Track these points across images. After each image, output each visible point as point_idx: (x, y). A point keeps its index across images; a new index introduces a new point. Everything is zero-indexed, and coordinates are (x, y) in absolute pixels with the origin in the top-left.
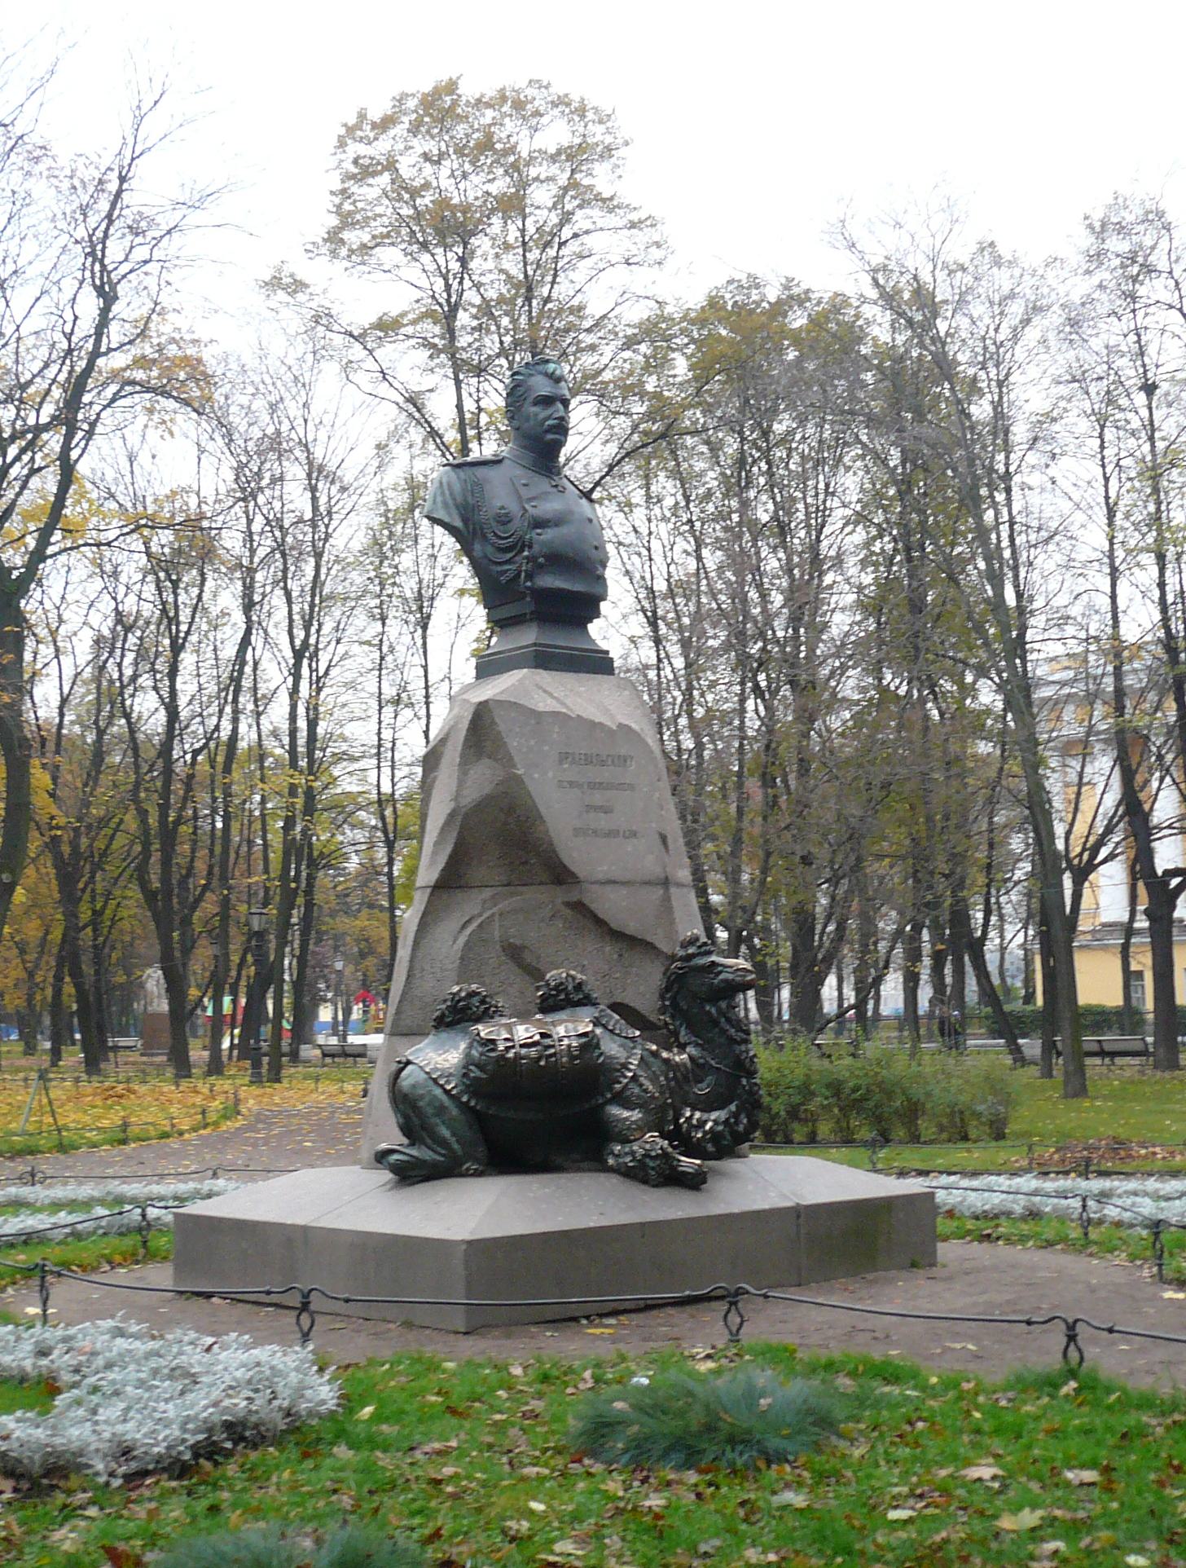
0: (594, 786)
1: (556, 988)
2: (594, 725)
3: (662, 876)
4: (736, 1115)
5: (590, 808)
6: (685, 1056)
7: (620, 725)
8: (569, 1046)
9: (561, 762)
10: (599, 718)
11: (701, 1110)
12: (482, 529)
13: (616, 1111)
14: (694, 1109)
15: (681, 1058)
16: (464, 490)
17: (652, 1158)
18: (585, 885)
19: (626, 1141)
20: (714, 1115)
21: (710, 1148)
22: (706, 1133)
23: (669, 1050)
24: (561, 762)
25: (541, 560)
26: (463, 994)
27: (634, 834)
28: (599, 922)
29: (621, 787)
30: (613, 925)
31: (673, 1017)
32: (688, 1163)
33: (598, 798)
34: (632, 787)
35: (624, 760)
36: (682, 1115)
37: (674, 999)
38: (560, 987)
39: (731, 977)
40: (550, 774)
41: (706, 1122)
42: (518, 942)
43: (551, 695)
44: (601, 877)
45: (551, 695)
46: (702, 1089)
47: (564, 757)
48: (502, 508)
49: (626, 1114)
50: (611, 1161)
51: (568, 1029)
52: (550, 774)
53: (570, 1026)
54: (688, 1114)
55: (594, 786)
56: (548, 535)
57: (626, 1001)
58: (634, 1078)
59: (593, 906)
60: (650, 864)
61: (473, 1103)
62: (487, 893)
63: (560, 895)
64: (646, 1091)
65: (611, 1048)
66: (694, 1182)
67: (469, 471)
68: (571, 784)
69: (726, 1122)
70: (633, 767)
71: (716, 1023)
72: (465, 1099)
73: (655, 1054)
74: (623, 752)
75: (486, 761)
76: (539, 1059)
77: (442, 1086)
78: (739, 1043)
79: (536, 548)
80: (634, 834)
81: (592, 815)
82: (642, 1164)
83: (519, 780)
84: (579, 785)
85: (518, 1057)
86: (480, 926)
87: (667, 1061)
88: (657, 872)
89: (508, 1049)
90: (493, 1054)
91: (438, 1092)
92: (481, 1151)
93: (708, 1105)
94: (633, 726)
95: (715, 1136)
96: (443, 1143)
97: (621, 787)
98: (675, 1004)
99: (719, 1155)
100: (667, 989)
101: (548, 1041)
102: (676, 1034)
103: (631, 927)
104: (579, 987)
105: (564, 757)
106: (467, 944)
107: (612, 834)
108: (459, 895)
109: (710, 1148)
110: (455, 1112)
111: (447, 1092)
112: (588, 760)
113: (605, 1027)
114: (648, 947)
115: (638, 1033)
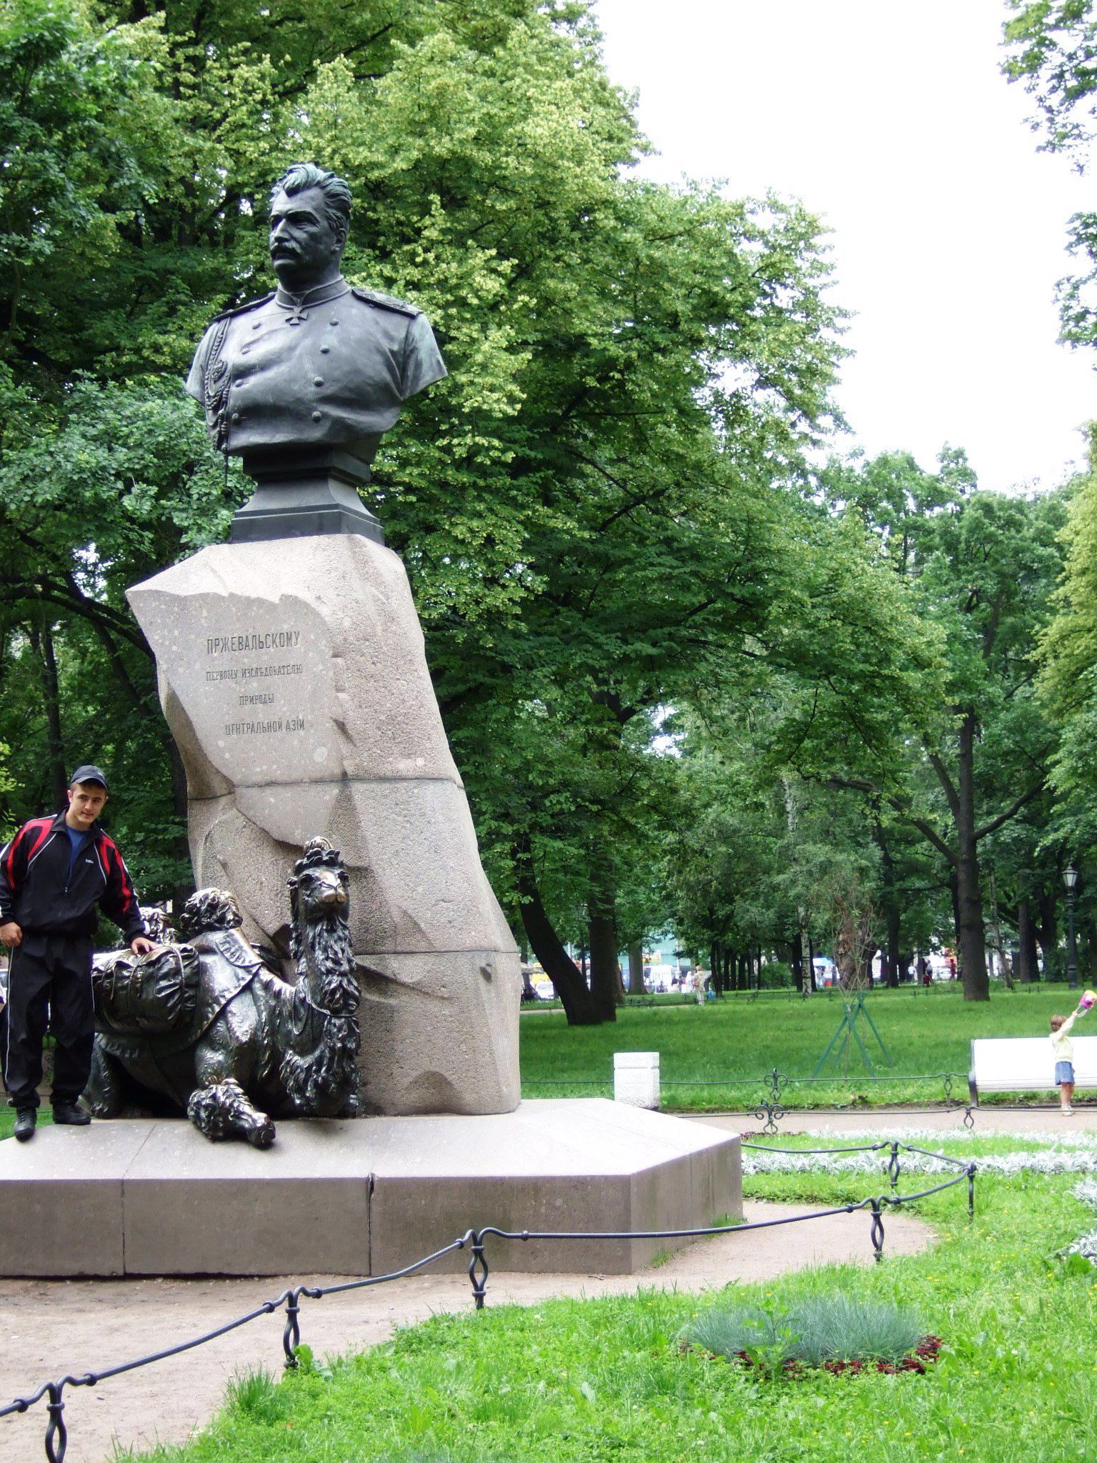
0: (248, 672)
2: (249, 602)
3: (337, 771)
4: (319, 1062)
7: (285, 598)
9: (210, 651)
14: (296, 1053)
18: (238, 790)
24: (210, 651)
25: (235, 416)
33: (254, 686)
36: (284, 1057)
40: (197, 666)
47: (213, 644)
52: (197, 666)
55: (248, 672)
56: (252, 382)
62: (223, 801)
65: (223, 978)
66: (263, 1141)
68: (223, 675)
70: (299, 646)
73: (267, 986)
74: (286, 628)
79: (231, 402)
81: (248, 707)
104: (213, 906)
105: (213, 644)
107: (270, 727)
112: (242, 644)
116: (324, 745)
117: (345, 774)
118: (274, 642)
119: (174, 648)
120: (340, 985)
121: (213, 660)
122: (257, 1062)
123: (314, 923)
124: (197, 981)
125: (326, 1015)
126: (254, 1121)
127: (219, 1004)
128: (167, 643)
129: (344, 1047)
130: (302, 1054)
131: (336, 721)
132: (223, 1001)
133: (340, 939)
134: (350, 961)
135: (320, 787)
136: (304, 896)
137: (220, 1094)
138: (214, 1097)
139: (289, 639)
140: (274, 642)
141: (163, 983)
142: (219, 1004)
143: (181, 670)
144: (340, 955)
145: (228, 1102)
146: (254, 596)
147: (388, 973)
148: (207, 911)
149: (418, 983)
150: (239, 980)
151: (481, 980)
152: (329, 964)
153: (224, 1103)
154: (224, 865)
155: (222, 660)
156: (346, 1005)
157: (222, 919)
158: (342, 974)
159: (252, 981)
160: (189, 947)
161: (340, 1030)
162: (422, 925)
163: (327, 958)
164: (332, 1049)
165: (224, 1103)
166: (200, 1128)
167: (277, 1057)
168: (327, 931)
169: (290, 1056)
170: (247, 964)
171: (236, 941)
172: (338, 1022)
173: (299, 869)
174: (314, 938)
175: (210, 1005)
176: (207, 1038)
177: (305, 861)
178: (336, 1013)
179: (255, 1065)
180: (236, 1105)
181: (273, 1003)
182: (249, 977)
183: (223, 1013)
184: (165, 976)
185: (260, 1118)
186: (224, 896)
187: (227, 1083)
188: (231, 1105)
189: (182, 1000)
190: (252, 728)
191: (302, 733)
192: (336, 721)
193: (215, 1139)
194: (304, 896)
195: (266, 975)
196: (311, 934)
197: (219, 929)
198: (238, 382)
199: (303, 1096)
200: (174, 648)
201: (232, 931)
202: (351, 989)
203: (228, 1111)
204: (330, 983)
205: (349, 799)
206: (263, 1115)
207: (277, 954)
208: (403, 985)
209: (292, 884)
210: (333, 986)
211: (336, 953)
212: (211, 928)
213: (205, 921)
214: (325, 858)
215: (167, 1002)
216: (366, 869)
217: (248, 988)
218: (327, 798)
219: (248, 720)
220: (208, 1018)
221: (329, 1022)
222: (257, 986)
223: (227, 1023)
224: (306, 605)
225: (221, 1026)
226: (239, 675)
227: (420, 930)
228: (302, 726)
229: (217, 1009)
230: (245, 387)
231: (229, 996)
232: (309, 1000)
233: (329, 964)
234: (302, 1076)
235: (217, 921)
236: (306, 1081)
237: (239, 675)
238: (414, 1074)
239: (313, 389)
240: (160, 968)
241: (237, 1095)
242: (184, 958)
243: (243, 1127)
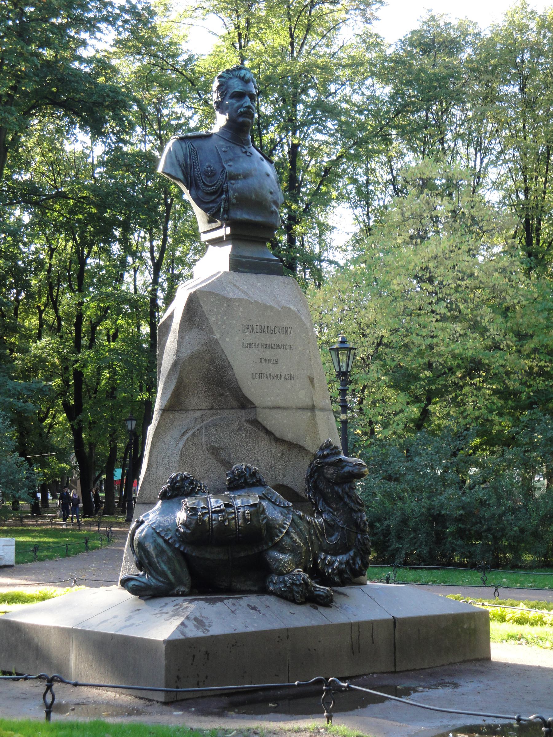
0: (265, 346)
1: (239, 475)
2: (266, 307)
4: (354, 558)
5: (262, 360)
6: (321, 520)
7: (283, 308)
8: (244, 513)
9: (244, 331)
10: (270, 303)
11: (331, 555)
12: (196, 181)
13: (276, 554)
14: (327, 553)
15: (319, 521)
16: (185, 156)
17: (296, 585)
18: (258, 410)
19: (281, 574)
20: (339, 558)
21: (337, 579)
22: (333, 570)
23: (312, 515)
24: (244, 331)
26: (178, 478)
27: (292, 377)
28: (268, 433)
29: (282, 347)
30: (278, 435)
31: (314, 495)
32: (322, 589)
33: (268, 354)
34: (291, 347)
35: (286, 330)
37: (315, 482)
38: (241, 474)
39: (351, 469)
40: (237, 338)
41: (334, 562)
42: (217, 445)
43: (238, 288)
44: (269, 404)
45: (238, 288)
47: (246, 327)
48: (209, 166)
49: (281, 556)
50: (271, 587)
51: (244, 501)
52: (237, 338)
53: (245, 499)
55: (265, 346)
57: (285, 483)
58: (288, 533)
59: (264, 423)
60: (302, 397)
61: (182, 549)
63: (243, 415)
64: (295, 542)
65: (274, 514)
67: (188, 142)
69: (347, 562)
71: (341, 499)
72: (177, 546)
74: (285, 324)
75: (196, 330)
76: (224, 521)
77: (163, 538)
78: (356, 512)
80: (292, 377)
81: (264, 364)
82: (291, 590)
83: (216, 342)
84: (256, 346)
85: (211, 520)
86: (193, 434)
87: (309, 523)
88: (307, 402)
89: (204, 514)
90: (195, 518)
91: (160, 541)
92: (187, 579)
93: (335, 551)
94: (293, 308)
95: (340, 572)
96: (163, 574)
97: (282, 347)
98: (316, 487)
99: (343, 583)
100: (311, 476)
101: (231, 510)
102: (316, 505)
103: (290, 436)
104: (254, 474)
105: (246, 327)
106: (184, 446)
107: (276, 377)
108: (180, 415)
109: (337, 579)
110: (170, 553)
111: (166, 541)
112: (262, 329)
113: (269, 500)
114: (300, 448)
115: (291, 504)
116: (304, 389)
117: (313, 405)
118: (279, 331)
119: (224, 327)
121: (246, 336)
126: (328, 591)
127: (284, 528)
128: (220, 323)
131: (309, 377)
135: (301, 412)
138: (303, 579)
139: (287, 330)
140: (279, 331)
142: (284, 528)
143: (227, 339)
146: (268, 304)
148: (250, 475)
155: (250, 338)
187: (299, 571)
190: (266, 376)
191: (293, 381)
192: (309, 377)
193: (301, 603)
197: (258, 486)
198: (233, 182)
200: (224, 327)
205: (315, 419)
209: (318, 463)
212: (253, 485)
217: (293, 520)
218: (305, 417)
219: (264, 372)
224: (296, 314)
226: (260, 346)
228: (293, 378)
229: (285, 531)
230: (234, 186)
237: (260, 346)
239: (270, 195)
243: (319, 596)
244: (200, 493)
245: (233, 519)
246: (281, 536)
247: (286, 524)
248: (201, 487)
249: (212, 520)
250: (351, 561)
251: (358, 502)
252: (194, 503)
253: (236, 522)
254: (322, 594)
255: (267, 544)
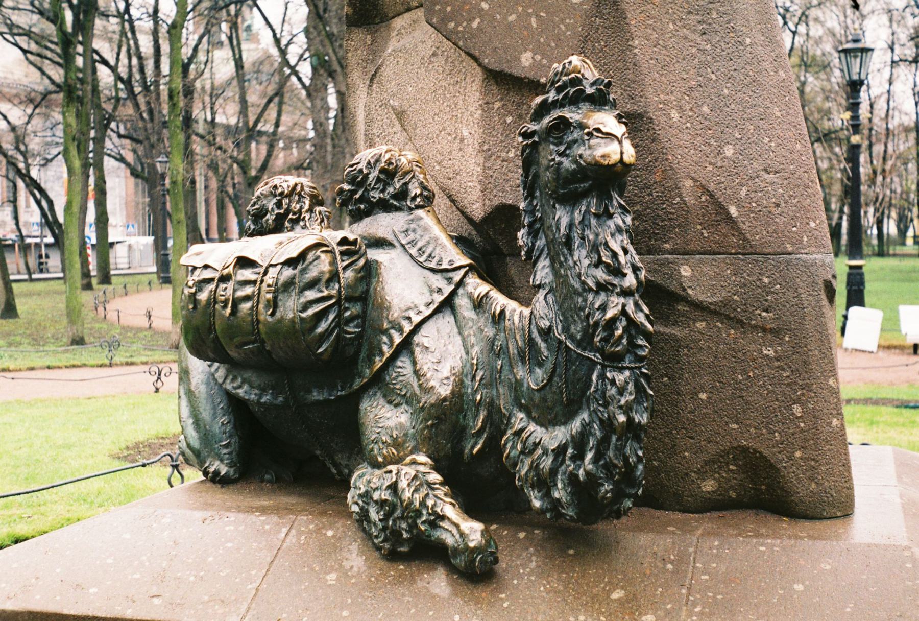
4: (579, 442)
19: (376, 465)
46: (533, 379)
54: (518, 427)
65: (404, 288)
69: (560, 451)
73: (479, 304)
85: (213, 300)
95: (544, 483)
101: (247, 274)
104: (389, 174)
120: (623, 312)
122: (464, 429)
123: (571, 200)
124: (363, 293)
125: (595, 363)
127: (400, 330)
129: (630, 420)
130: (547, 422)
132: (408, 328)
133: (619, 230)
134: (635, 269)
136: (550, 153)
137: (403, 484)
138: (393, 487)
141: (311, 295)
144: (622, 259)
145: (418, 497)
147: (673, 286)
148: (378, 180)
149: (726, 303)
150: (432, 291)
151: (823, 296)
152: (601, 274)
153: (411, 502)
154: (400, 115)
156: (633, 346)
157: (402, 194)
158: (626, 293)
159: (453, 293)
160: (351, 237)
161: (621, 391)
162: (733, 211)
163: (599, 263)
164: (608, 425)
165: (411, 502)
166: (369, 536)
167: (497, 424)
168: (597, 216)
169: (519, 419)
170: (445, 266)
171: (426, 229)
172: (620, 378)
173: (544, 109)
174: (571, 226)
175: (385, 332)
176: (379, 382)
177: (552, 96)
178: (614, 360)
179: (459, 434)
180: (430, 503)
181: (490, 331)
182: (448, 289)
183: (407, 345)
184: (313, 284)
185: (473, 531)
186: (406, 158)
187: (414, 462)
188: (423, 503)
189: (340, 322)
193: (393, 556)
194: (550, 153)
195: (477, 286)
196: (564, 222)
199: (547, 495)
201: (420, 213)
202: (640, 318)
203: (418, 513)
204: (603, 308)
206: (479, 526)
207: (492, 247)
208: (698, 306)
209: (526, 135)
210: (610, 314)
211: (615, 255)
212: (385, 206)
213: (376, 195)
214: (589, 91)
215: (315, 326)
216: (641, 116)
217: (448, 304)
220: (382, 353)
221: (602, 376)
222: (462, 302)
223: (414, 363)
225: (404, 364)
227: (729, 217)
229: (398, 339)
231: (416, 319)
232: (558, 333)
233: (601, 274)
234: (547, 463)
235: (395, 196)
236: (553, 472)
238: (713, 449)
240: (303, 271)
241: (430, 485)
242: (342, 253)
244: (298, 228)
245: (247, 298)
246: (387, 351)
247: (409, 318)
248: (300, 211)
249: (215, 302)
250: (570, 451)
251: (600, 257)
252: (198, 254)
253: (253, 307)
254: (450, 541)
255: (361, 376)
